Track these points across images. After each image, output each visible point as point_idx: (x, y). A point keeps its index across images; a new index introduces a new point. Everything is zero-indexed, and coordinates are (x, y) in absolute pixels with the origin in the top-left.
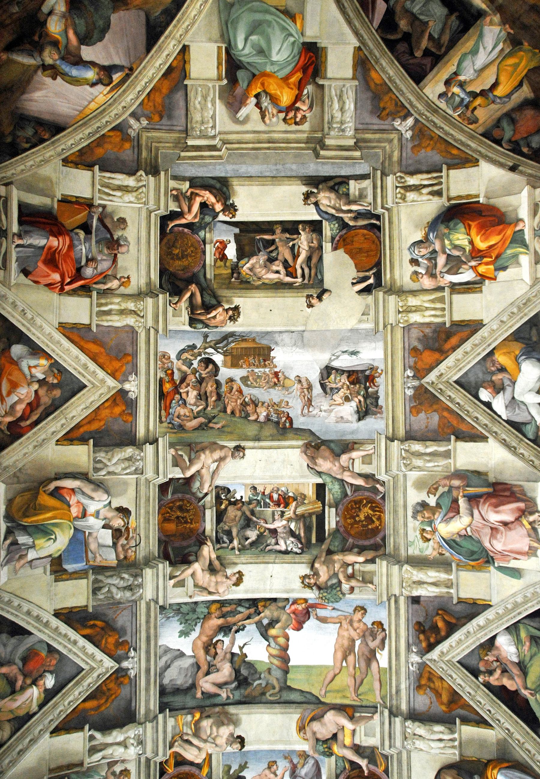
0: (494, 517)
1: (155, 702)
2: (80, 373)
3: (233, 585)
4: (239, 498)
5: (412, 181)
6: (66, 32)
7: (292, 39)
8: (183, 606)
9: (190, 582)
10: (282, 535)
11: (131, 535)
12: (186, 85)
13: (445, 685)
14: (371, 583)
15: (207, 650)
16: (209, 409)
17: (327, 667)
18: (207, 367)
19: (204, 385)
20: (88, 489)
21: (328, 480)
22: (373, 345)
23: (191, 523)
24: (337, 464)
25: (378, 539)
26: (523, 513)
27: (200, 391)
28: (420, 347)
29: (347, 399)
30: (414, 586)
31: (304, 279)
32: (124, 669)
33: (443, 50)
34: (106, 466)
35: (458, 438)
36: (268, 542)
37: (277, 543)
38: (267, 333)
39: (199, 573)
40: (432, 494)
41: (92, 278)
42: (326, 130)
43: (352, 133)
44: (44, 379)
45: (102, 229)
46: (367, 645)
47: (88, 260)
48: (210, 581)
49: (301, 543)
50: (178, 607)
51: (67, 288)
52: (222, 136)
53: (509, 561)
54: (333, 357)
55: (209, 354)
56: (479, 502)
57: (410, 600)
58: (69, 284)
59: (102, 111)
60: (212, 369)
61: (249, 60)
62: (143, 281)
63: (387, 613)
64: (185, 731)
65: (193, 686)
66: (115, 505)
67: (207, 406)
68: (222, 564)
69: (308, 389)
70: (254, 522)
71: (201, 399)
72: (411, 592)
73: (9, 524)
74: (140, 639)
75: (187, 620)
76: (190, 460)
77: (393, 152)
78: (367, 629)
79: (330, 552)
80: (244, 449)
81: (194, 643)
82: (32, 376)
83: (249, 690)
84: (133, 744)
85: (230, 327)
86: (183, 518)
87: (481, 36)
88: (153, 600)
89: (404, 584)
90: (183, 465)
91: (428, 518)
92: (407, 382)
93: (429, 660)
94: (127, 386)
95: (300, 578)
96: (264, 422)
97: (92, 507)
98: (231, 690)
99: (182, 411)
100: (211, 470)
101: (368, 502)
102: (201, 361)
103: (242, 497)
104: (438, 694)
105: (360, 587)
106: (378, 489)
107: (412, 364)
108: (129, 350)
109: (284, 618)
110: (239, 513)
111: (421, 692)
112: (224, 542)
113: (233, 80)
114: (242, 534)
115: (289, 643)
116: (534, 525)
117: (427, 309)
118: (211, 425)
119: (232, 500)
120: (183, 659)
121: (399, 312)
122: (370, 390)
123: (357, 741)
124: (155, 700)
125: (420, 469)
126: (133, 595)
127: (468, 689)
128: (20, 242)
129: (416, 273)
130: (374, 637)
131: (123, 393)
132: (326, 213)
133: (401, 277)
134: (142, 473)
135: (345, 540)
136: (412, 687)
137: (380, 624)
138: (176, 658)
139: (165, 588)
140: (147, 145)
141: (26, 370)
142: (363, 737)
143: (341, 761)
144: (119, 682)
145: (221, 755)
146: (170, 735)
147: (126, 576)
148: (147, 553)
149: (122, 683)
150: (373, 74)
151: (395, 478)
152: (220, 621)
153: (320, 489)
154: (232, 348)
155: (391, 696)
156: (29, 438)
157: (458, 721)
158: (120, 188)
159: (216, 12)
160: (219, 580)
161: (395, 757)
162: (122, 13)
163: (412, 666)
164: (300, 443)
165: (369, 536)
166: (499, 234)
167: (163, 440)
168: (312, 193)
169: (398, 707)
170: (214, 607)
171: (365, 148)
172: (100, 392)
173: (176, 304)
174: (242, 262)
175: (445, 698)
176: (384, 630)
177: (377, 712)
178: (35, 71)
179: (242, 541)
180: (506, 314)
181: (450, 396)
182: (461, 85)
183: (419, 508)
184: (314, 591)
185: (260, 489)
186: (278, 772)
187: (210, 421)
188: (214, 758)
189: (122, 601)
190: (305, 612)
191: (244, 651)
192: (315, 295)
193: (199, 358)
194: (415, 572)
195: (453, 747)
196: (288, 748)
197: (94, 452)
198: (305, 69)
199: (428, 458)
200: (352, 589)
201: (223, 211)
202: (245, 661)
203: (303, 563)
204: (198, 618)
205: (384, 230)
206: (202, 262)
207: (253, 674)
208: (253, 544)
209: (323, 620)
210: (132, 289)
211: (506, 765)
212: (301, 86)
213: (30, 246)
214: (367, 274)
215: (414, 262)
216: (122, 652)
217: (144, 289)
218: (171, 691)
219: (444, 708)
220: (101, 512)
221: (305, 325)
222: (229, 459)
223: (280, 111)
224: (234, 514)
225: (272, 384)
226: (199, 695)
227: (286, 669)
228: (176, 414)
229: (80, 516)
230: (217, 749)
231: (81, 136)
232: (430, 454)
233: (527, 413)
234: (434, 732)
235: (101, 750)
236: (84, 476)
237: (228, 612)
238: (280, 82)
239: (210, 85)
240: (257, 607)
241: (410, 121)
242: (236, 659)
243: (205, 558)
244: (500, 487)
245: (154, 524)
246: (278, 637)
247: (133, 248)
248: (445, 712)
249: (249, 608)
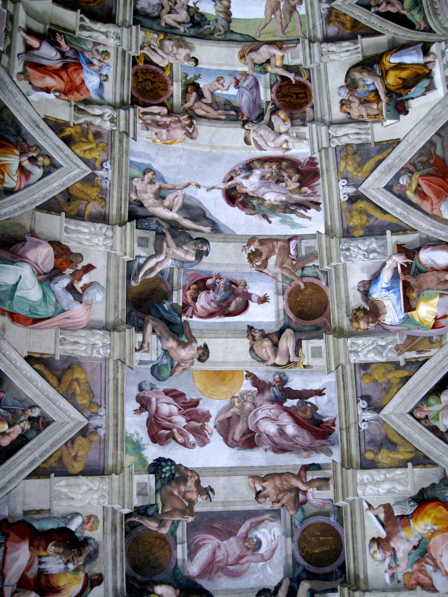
1: (130, 17)
13: (348, 18)
46: (290, 3)
65: (159, 17)
83: (201, 30)
84: (113, 37)
104: (343, 24)
111: (331, 25)
115: (231, 4)
123: (286, 63)
124: (130, 15)
127: (364, 17)
142: (290, 60)
143: (274, 77)
145: (180, 66)
155: (309, 31)
157: (359, 37)
161: (315, 69)
169: (315, 37)
175: (348, 25)
177: (299, 42)
186: (225, 84)
188: (174, 66)
191: (197, 5)
195: (358, 53)
196: (233, 69)
202: (197, 12)
207: (204, 21)
211: (396, 50)
219: (348, 31)
226: (163, 24)
227: (229, 19)
230: (177, 61)
234: (343, 47)
235: (88, 31)
242: (191, 10)
248: (349, 34)
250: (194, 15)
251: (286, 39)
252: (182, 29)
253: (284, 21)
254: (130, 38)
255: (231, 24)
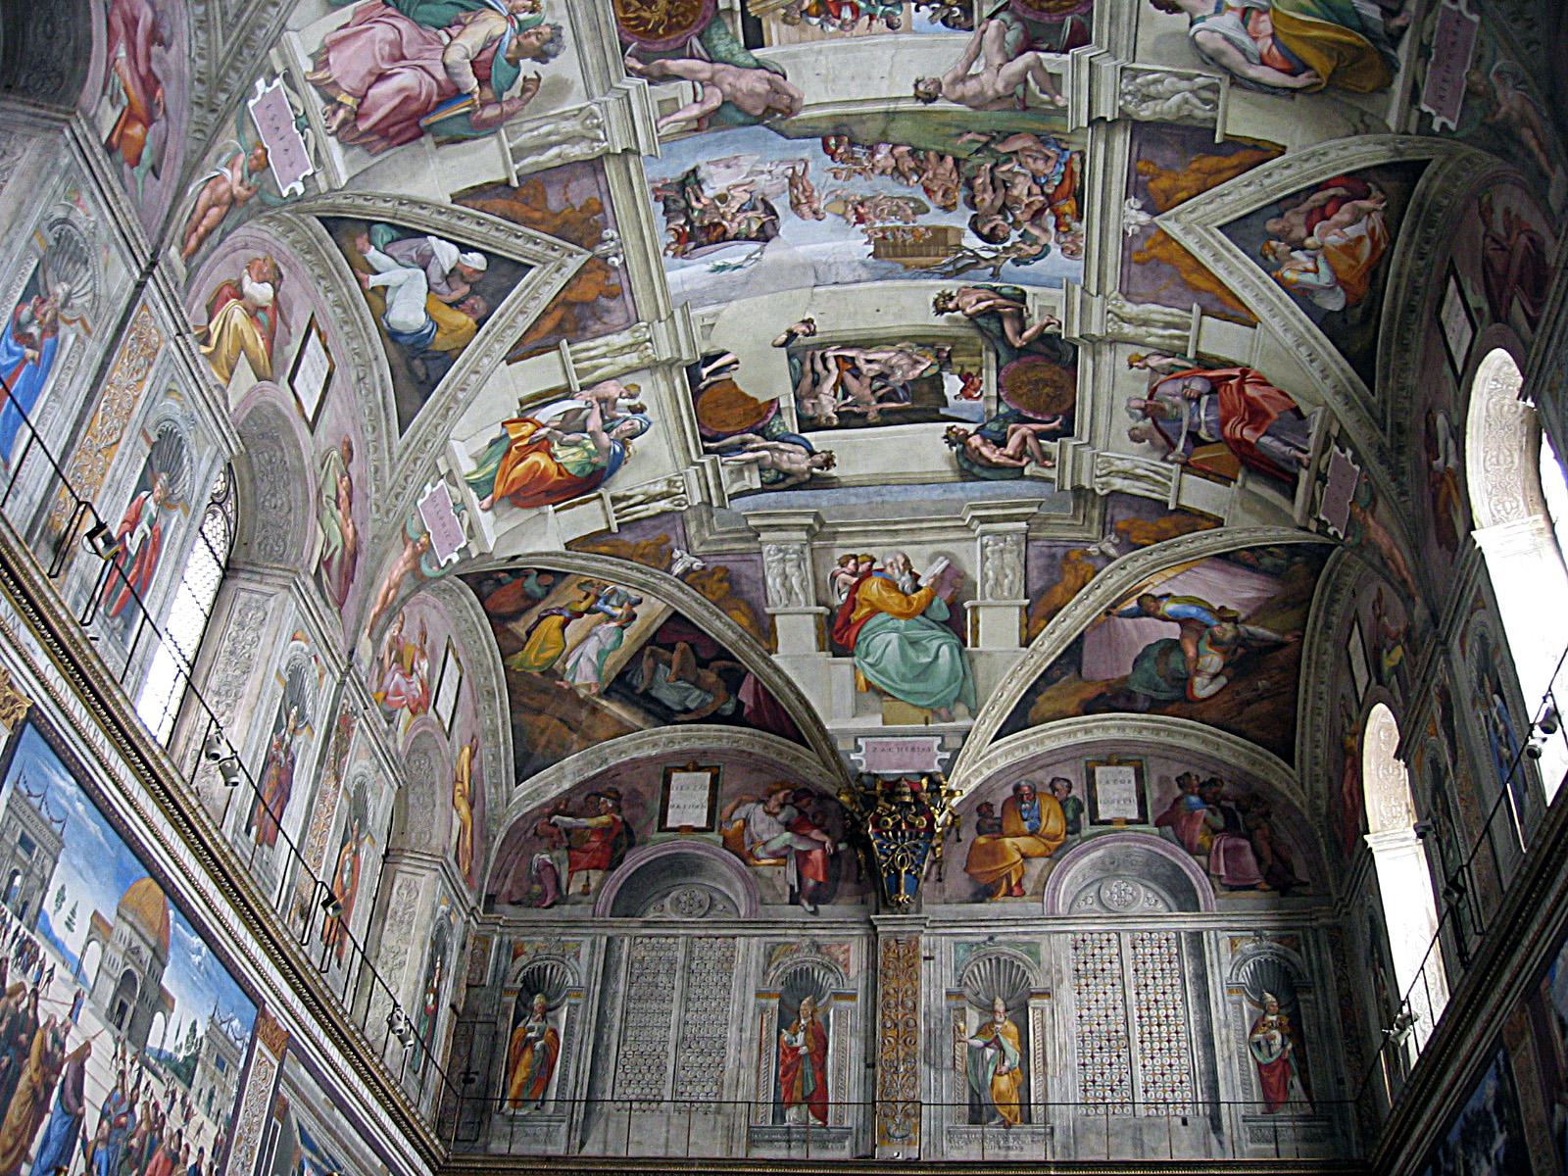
0: (406, 78)
2: (1229, 250)
4: (922, 8)
5: (664, 505)
6: (1198, 655)
7: (870, 660)
12: (1026, 597)
16: (989, 166)
18: (993, 229)
19: (999, 203)
20: (1234, 58)
21: (741, 58)
22: (687, 287)
24: (727, 88)
26: (358, 115)
27: (1006, 195)
28: (603, 301)
29: (723, 198)
31: (823, 356)
33: (647, 651)
34: (1192, 91)
35: (507, 183)
38: (882, 279)
40: (532, 80)
41: (1193, 376)
42: (807, 550)
43: (765, 549)
44: (1293, 250)
45: (1170, 434)
47: (1198, 400)
51: (1236, 372)
52: (971, 535)
53: (355, 14)
54: (757, 255)
55: (990, 250)
56: (439, 95)
58: (1233, 377)
59: (1155, 567)
60: (985, 224)
61: (929, 632)
62: (1107, 356)
66: (1185, 17)
67: (991, 169)
69: (799, 203)
71: (1004, 182)
73: (1392, 52)
76: (1026, 81)
77: (698, 531)
80: (917, 97)
82: (1315, 258)
85: (951, 285)
87: (598, 672)
90: (1040, 75)
91: (529, 35)
92: (617, 247)
94: (1144, 218)
96: (879, 143)
97: (1229, 22)
99: (1040, 165)
100: (983, 61)
101: (655, 30)
102: (1005, 239)
103: (917, 9)
106: (639, 61)
107: (613, 275)
108: (1135, 268)
113: (955, 606)
116: (334, 105)
117: (604, 356)
118: (984, 139)
119: (937, 5)
121: (650, 340)
122: (682, 222)
125: (564, 117)
128: (1300, 455)
129: (632, 397)
131: (1153, 208)
132: (794, 443)
133: (655, 385)
134: (1123, 69)
140: (1091, 523)
141: (1322, 267)
150: (745, 622)
151: (608, 87)
153: (755, 37)
154: (947, 256)
156: (1334, 170)
158: (1138, 478)
159: (980, 689)
162: (1117, 675)
164: (803, 115)
166: (513, 480)
167: (1078, 122)
168: (822, 468)
171: (743, 531)
172: (1193, 216)
173: (1049, 324)
174: (935, 369)
178: (1248, 617)
180: (473, 386)
181: (536, 244)
182: (612, 618)
183: (551, 47)
185: (880, 25)
187: (986, 144)
192: (800, 336)
193: (1008, 244)
197: (1215, 121)
198: (847, 623)
199: (553, 138)
201: (967, 436)
205: (695, 437)
206: (1003, 373)
210: (1125, 352)
212: (852, 603)
213: (1288, 444)
214: (713, 379)
215: (639, 410)
217: (1105, 349)
220: (1212, 10)
221: (813, 295)
222: (946, 80)
223: (881, 571)
225: (867, 204)
228: (1051, 163)
229: (1254, 14)
231: (1191, 546)
232: (552, 145)
233: (395, 254)
236: (1238, 81)
238: (879, 605)
239: (989, 600)
241: (678, 569)
244: (408, 135)
247: (1121, 402)
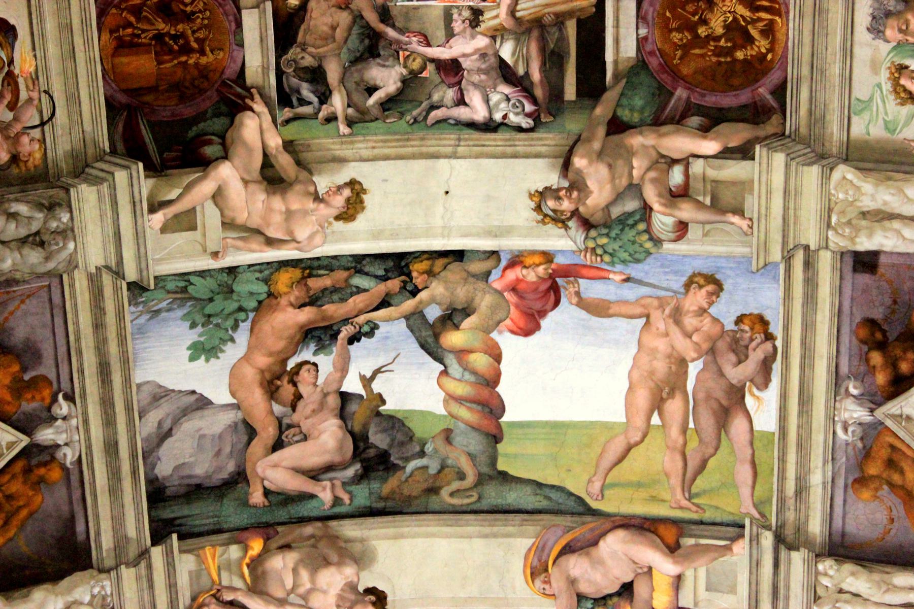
1: (138, 520)
3: (338, 218)
8: (193, 279)
9: (210, 216)
10: (476, 78)
11: (23, 95)
14: (739, 211)
15: (271, 388)
17: (607, 426)
23: (202, 52)
25: (763, 91)
30: (864, 223)
32: (46, 448)
36: (436, 97)
37: (461, 101)
39: (236, 192)
46: (721, 374)
48: (269, 210)
49: (534, 101)
50: (182, 284)
57: (849, 261)
63: (781, 294)
64: (225, 583)
65: (240, 478)
68: (299, 163)
70: (391, 43)
72: (852, 240)
74: (81, 371)
75: (209, 316)
78: (723, 332)
79: (617, 127)
81: (234, 373)
83: (393, 482)
86: (175, 38)
88: (107, 267)
89: (834, 219)
93: (893, 417)
95: (531, 196)
98: (344, 484)
105: (704, 223)
109: (485, 302)
110: (344, 18)
111: (866, 494)
112: (303, 102)
114: (356, 77)
115: (503, 367)
120: (206, 412)
124: (138, 514)
126: (47, 259)
130: (740, 352)
135: (663, 93)
136: (841, 482)
137: (762, 322)
138: (185, 412)
139: (139, 236)
142: (702, 593)
144: (33, 477)
146: (188, 595)
147: (22, 209)
148: (79, 144)
149: (42, 480)
152: (306, 315)
155: (782, 501)
160: (295, 206)
163: (845, 430)
165: (736, 82)
169: (800, 528)
170: (284, 279)
176: (769, 337)
177: (742, 536)
179: (356, 97)
184: (572, 232)
189: (18, 276)
190: (544, 287)
191: (376, 387)
194: (867, 187)
200: (682, 228)
202: (378, 414)
203: (537, 156)
204: (241, 309)
207: (402, 444)
208: (388, 104)
209: (599, 309)
216: (34, 405)
218: (182, 490)
224: (328, 20)
226: (257, 497)
227: (494, 431)
237: (324, 290)
240: (409, 275)
242: (353, 407)
243: (250, 150)
245: (90, 61)
246: (471, 351)
249: (384, 279)
250: (366, 426)
251: (695, 516)
252: (325, 494)
253: (693, 444)
254: (146, 597)
255: (498, 445)
